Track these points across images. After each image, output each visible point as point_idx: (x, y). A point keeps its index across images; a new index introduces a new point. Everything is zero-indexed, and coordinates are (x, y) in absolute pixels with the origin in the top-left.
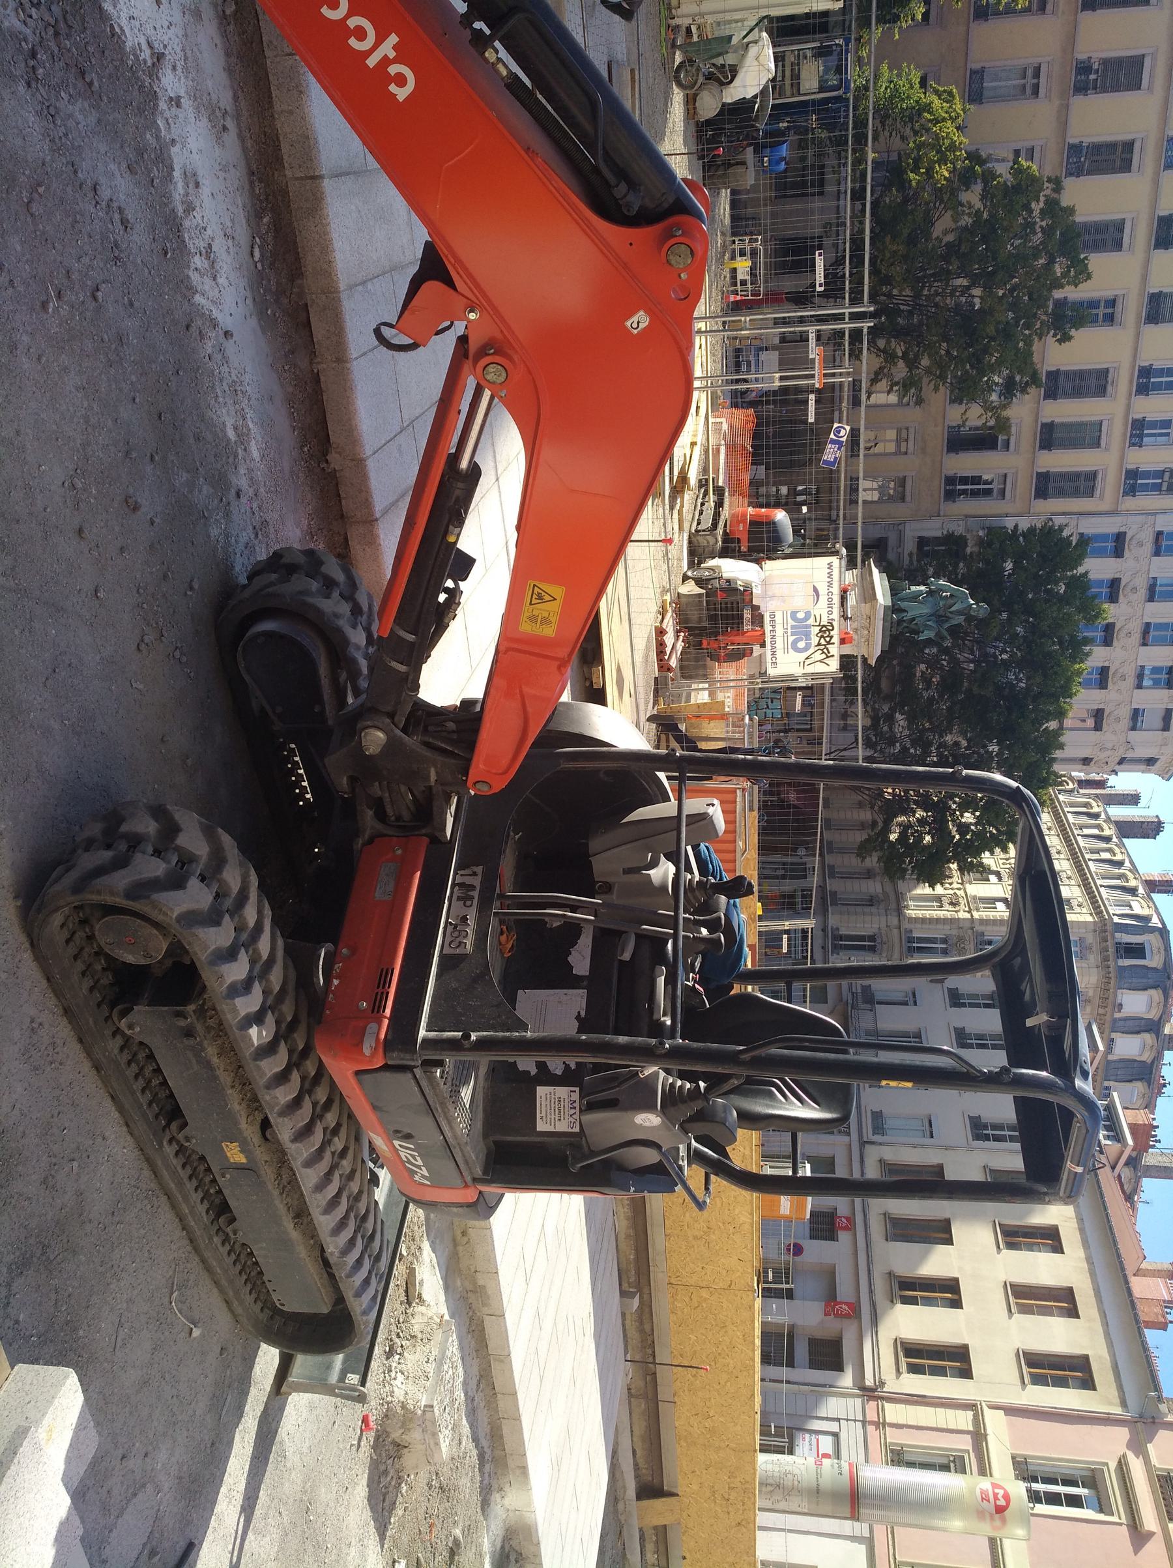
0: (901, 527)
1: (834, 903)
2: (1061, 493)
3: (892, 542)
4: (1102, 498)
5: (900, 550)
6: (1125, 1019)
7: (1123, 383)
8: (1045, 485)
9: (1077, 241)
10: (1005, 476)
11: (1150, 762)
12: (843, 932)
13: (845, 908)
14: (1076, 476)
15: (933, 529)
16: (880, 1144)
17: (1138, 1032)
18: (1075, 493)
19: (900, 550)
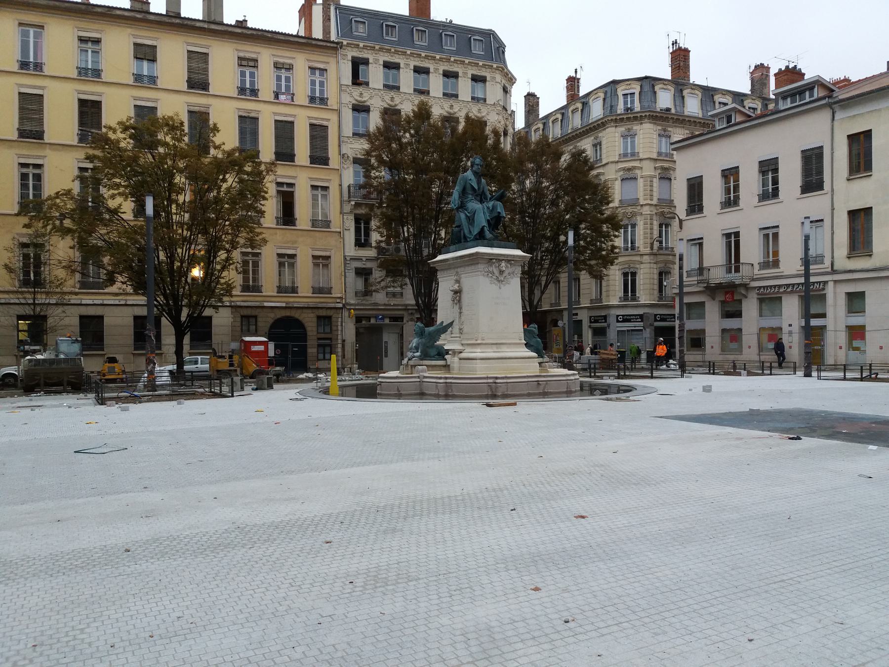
0: (348, 258)
1: (601, 300)
2: (325, 148)
3: (359, 265)
4: (328, 120)
5: (364, 259)
6: (675, 105)
7: (249, 106)
8: (319, 158)
9: (145, 125)
10: (312, 186)
11: (506, 91)
12: (622, 294)
13: (604, 294)
14: (312, 138)
15: (350, 237)
16: (833, 257)
17: (683, 97)
18: (325, 138)
19: (364, 259)
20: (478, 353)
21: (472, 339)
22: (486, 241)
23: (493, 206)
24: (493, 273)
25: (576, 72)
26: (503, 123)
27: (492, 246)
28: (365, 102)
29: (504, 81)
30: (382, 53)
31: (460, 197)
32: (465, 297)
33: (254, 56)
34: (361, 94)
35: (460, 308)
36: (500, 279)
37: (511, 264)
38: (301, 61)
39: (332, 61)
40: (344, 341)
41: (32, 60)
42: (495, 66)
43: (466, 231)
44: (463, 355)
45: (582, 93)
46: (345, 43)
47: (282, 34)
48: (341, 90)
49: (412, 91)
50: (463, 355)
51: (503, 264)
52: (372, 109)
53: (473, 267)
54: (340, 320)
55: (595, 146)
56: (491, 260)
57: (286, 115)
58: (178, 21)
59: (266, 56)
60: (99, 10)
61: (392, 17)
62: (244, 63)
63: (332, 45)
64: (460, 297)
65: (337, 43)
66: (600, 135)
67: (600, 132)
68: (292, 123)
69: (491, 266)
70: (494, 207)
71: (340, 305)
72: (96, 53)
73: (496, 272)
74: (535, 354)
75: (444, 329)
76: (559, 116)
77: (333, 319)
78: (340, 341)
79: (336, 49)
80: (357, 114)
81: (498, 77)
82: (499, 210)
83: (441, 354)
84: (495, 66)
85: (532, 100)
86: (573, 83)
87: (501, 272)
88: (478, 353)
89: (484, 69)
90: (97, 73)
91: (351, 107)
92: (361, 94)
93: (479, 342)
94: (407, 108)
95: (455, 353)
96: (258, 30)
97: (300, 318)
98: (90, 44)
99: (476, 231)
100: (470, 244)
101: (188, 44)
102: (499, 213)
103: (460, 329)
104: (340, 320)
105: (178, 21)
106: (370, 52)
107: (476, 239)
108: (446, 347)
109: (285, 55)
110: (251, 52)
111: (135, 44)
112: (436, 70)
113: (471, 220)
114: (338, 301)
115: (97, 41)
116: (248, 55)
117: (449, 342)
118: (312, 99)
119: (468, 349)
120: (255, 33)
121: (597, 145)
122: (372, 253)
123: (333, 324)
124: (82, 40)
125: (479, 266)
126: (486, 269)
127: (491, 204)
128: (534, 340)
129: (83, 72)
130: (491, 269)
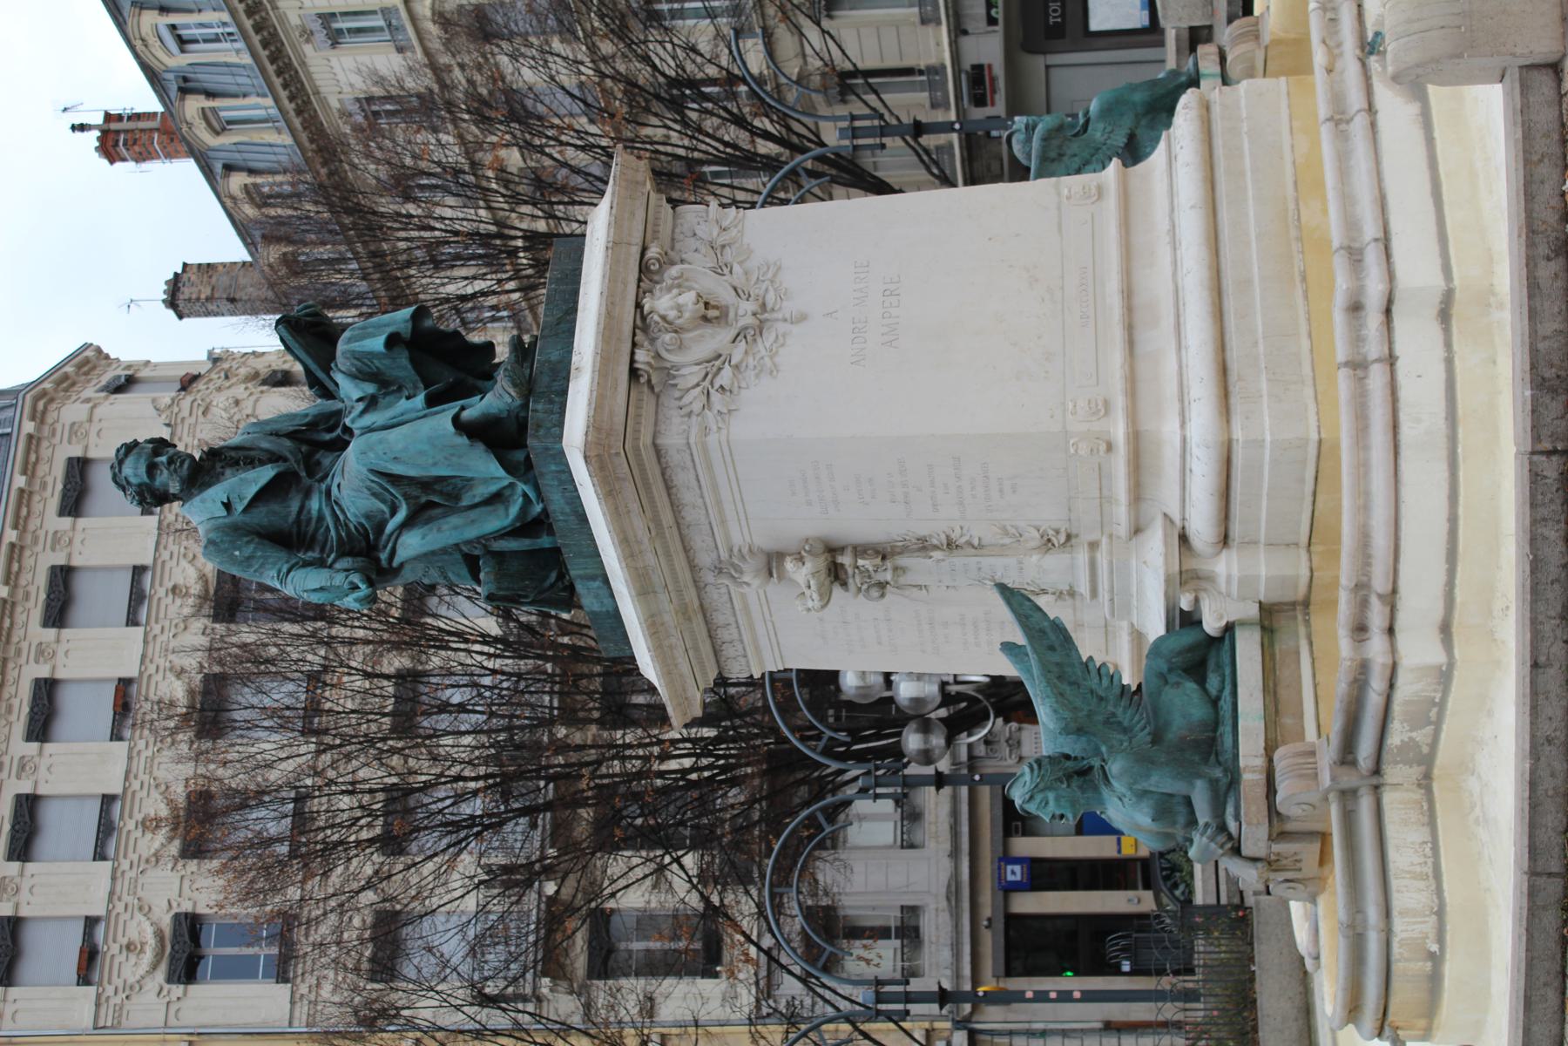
11: (125, 384)
20: (1187, 432)
21: (1103, 475)
22: (538, 407)
23: (360, 375)
25: (82, 128)
26: (239, 391)
28: (159, 935)
29: (89, 392)
31: (321, 563)
32: (857, 522)
34: (129, 947)
35: (924, 546)
37: (667, 261)
42: (29, 427)
43: (494, 521)
44: (1202, 527)
45: (146, 101)
48: (115, 1028)
49: (121, 748)
50: (1202, 527)
51: (661, 303)
52: (187, 907)
53: (682, 478)
55: (335, 38)
56: (640, 378)
64: (860, 550)
66: (294, 19)
67: (282, 19)
69: (669, 373)
70: (362, 374)
74: (1187, 100)
75: (1049, 639)
76: (237, 181)
80: (208, 966)
81: (71, 412)
82: (377, 344)
83: (1197, 654)
84: (29, 427)
85: (189, 293)
86: (119, 139)
88: (1187, 432)
89: (42, 469)
91: (178, 990)
92: (129, 947)
93: (1119, 432)
94: (167, 771)
95: (1187, 576)
99: (485, 469)
100: (557, 502)
102: (393, 341)
103: (1048, 544)
107: (523, 469)
108: (1156, 628)
112: (41, 653)
113: (430, 498)
117: (1121, 603)
119: (1166, 496)
121: (334, 30)
122: (743, 905)
125: (672, 439)
126: (694, 399)
127: (350, 390)
130: (691, 376)
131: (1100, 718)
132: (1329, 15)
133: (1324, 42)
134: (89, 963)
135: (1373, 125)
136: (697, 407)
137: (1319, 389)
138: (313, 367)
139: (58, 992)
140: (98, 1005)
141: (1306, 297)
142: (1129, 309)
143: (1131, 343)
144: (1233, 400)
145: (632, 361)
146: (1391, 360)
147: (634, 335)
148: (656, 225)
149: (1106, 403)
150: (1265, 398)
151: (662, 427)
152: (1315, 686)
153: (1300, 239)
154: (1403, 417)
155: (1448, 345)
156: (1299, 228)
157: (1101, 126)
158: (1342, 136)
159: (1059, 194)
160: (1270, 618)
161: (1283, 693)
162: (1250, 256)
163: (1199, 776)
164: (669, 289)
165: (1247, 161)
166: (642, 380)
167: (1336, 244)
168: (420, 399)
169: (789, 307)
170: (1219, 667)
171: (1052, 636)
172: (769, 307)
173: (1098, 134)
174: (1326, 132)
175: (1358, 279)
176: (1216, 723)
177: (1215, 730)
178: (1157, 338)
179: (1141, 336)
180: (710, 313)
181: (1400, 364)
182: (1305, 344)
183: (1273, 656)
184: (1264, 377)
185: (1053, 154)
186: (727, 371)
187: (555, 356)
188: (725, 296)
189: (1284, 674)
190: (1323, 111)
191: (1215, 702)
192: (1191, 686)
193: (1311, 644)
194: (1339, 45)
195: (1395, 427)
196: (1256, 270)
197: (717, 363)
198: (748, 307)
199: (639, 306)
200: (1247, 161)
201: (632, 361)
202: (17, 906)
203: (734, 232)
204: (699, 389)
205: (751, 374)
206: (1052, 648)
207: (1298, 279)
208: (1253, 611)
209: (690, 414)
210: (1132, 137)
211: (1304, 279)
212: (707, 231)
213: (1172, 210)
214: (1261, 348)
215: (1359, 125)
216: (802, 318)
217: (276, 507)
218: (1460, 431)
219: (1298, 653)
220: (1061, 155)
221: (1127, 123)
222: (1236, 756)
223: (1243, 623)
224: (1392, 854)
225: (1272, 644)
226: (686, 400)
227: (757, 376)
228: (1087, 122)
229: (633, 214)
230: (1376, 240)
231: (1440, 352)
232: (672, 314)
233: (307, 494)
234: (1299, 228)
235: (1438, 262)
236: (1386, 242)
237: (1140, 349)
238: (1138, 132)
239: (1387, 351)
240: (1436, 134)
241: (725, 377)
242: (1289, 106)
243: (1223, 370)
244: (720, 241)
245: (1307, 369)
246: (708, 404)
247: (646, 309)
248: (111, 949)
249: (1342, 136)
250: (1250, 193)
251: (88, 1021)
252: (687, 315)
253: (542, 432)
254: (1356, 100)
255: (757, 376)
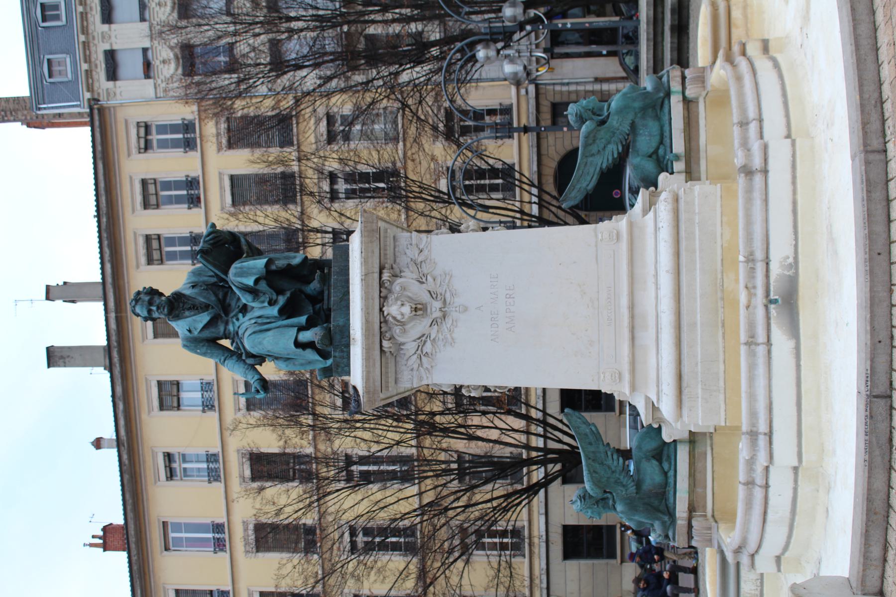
24: (422, 339)
27: (345, 330)
30: (91, 28)
33: (141, 241)
34: (164, 62)
36: (433, 309)
38: (135, 167)
39: (121, 115)
40: (598, 80)
41: (210, 535)
46: (88, 95)
47: (97, 201)
54: (558, 88)
57: (222, 188)
58: (115, 354)
59: (139, 223)
60: (125, 457)
61: (28, 9)
62: (156, 255)
63: (96, 117)
65: (91, 109)
68: (232, 178)
71: (532, 88)
72: (184, 458)
73: (420, 327)
77: (558, 99)
78: (597, 87)
79: (101, 110)
87: (419, 309)
90: (211, 458)
92: (164, 62)
96: (100, 237)
97: (557, 158)
98: (175, 465)
101: (144, 337)
104: (558, 88)
105: (115, 354)
106: (93, 49)
109: (130, 195)
110: (136, 244)
111: (162, 407)
114: (523, 92)
115: (169, 457)
116: (142, 251)
118: (189, 145)
120: (106, 243)
123: (565, 99)
124: (171, 474)
128: (613, 122)
129: (213, 476)
130: (410, 347)
131: (612, 480)
132: (751, 265)
133: (747, 287)
134: (148, 66)
135: (769, 352)
136: (415, 366)
137: (728, 396)
138: (219, 273)
139: (137, 82)
140: (155, 88)
141: (724, 337)
142: (632, 317)
143: (633, 339)
144: (683, 397)
145: (381, 346)
146: (767, 486)
147: (381, 327)
148: (385, 250)
149: (620, 374)
150: (700, 400)
151: (399, 376)
152: (713, 472)
153: (722, 299)
154: (769, 511)
155: (796, 481)
156: (722, 291)
157: (616, 117)
158: (752, 354)
159: (596, 236)
160: (693, 439)
161: (698, 475)
162: (697, 310)
163: (658, 519)
164: (397, 299)
165: (697, 242)
166: (388, 354)
167: (744, 428)
168: (274, 311)
169: (458, 301)
170: (669, 457)
171: (591, 437)
172: (448, 302)
173: (615, 123)
174: (743, 349)
175: (754, 450)
176: (666, 484)
177: (665, 488)
178: (647, 338)
179: (639, 334)
180: (419, 309)
181: (771, 490)
182: (722, 367)
183: (694, 457)
184: (700, 386)
185: (590, 141)
186: (429, 344)
187: (341, 322)
188: (426, 298)
189: (699, 465)
190: (743, 338)
191: (666, 474)
192: (655, 462)
193: (712, 449)
194: (754, 287)
195: (765, 513)
196: (699, 316)
197: (424, 338)
198: (437, 305)
199: (381, 310)
200: (697, 242)
201: (381, 346)
202: (111, 45)
203: (426, 252)
204: (416, 356)
205: (440, 343)
206: (590, 444)
207: (720, 325)
208: (686, 435)
209: (412, 370)
210: (633, 125)
211: (723, 326)
212: (413, 253)
213: (656, 262)
214: (699, 367)
215: (761, 350)
216: (466, 309)
217: (213, 330)
218: (797, 518)
219: (706, 454)
220: (594, 141)
221: (630, 117)
222: (675, 508)
223: (681, 441)
224: (742, 585)
225: (694, 449)
226: (410, 362)
227: (444, 345)
228: (609, 114)
229: (373, 252)
230: (765, 434)
231: (791, 484)
232: (399, 317)
233: (227, 323)
234: (722, 291)
235: (796, 449)
236: (770, 435)
237: (637, 342)
238: (637, 120)
239: (765, 482)
240: (802, 363)
241: (428, 348)
242: (722, 206)
243: (680, 377)
244: (420, 259)
245: (722, 383)
246: (421, 365)
247: (385, 313)
248: (156, 63)
249: (752, 354)
250: (698, 266)
251: (153, 95)
252: (406, 317)
253: (340, 370)
254: (761, 337)
255: (444, 345)
